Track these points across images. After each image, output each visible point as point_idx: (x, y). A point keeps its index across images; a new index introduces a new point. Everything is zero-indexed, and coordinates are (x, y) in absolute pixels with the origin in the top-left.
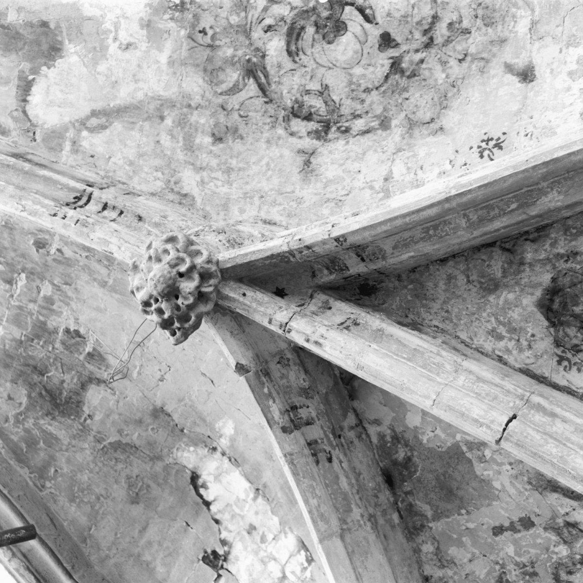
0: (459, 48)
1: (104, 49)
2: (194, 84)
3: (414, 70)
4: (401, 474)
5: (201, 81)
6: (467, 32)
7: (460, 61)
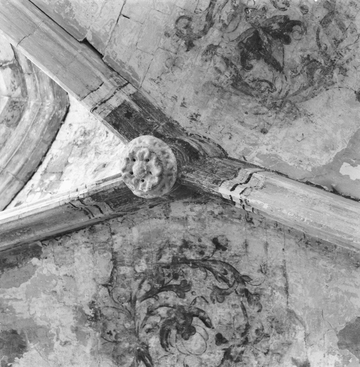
1: (51, 345)
3: (238, 358)
5: (111, 363)
6: (267, 336)
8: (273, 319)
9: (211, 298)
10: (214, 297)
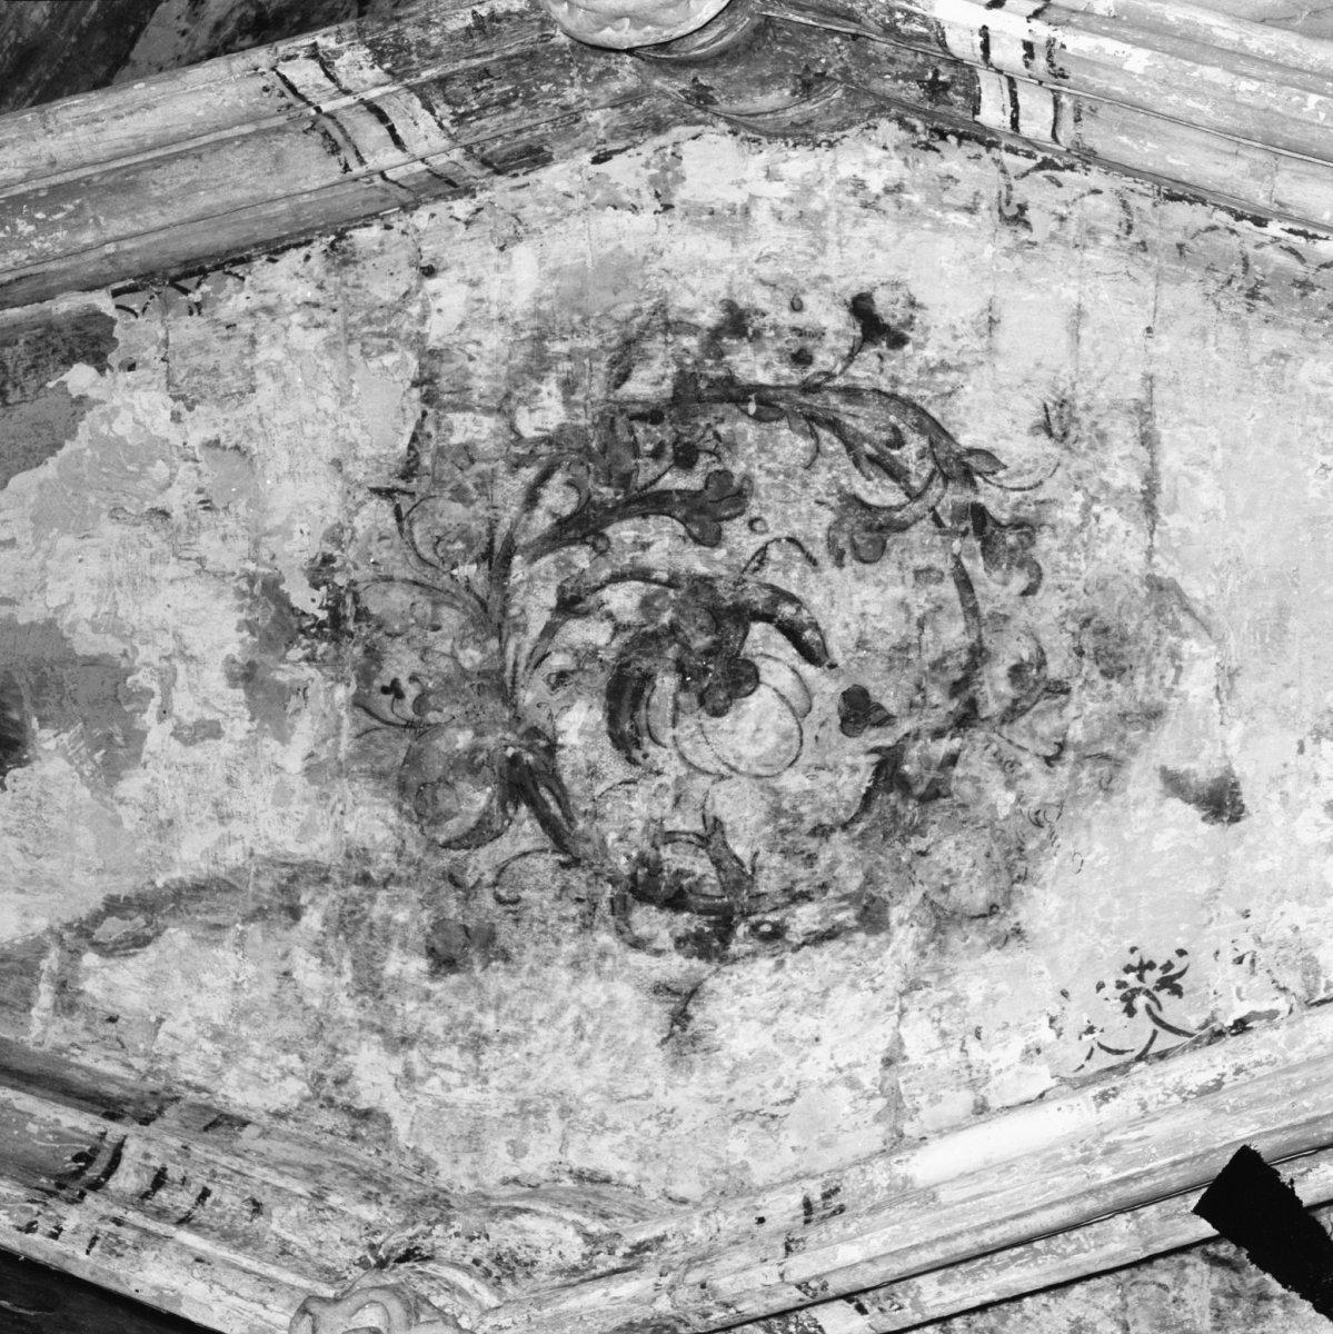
0: (1044, 728)
1: (136, 738)
2: (372, 821)
6: (1059, 689)
7: (1049, 760)
8: (1087, 622)
9: (831, 542)
10: (843, 541)
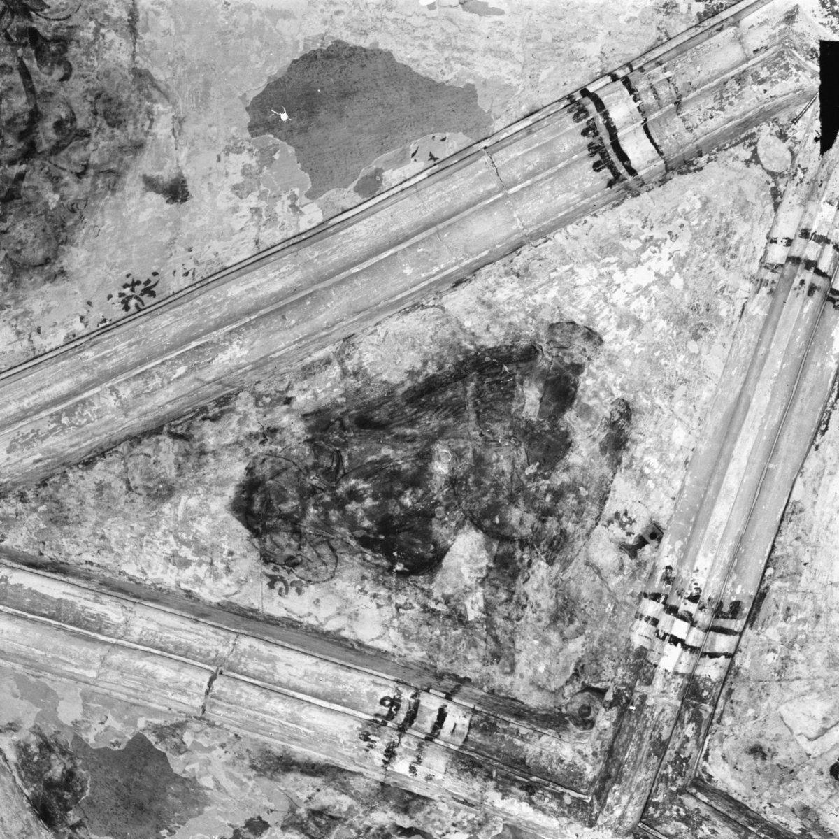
0: (75, 157)
3: (10, 191)
4: (60, 799)
6: (84, 134)
8: (99, 96)
